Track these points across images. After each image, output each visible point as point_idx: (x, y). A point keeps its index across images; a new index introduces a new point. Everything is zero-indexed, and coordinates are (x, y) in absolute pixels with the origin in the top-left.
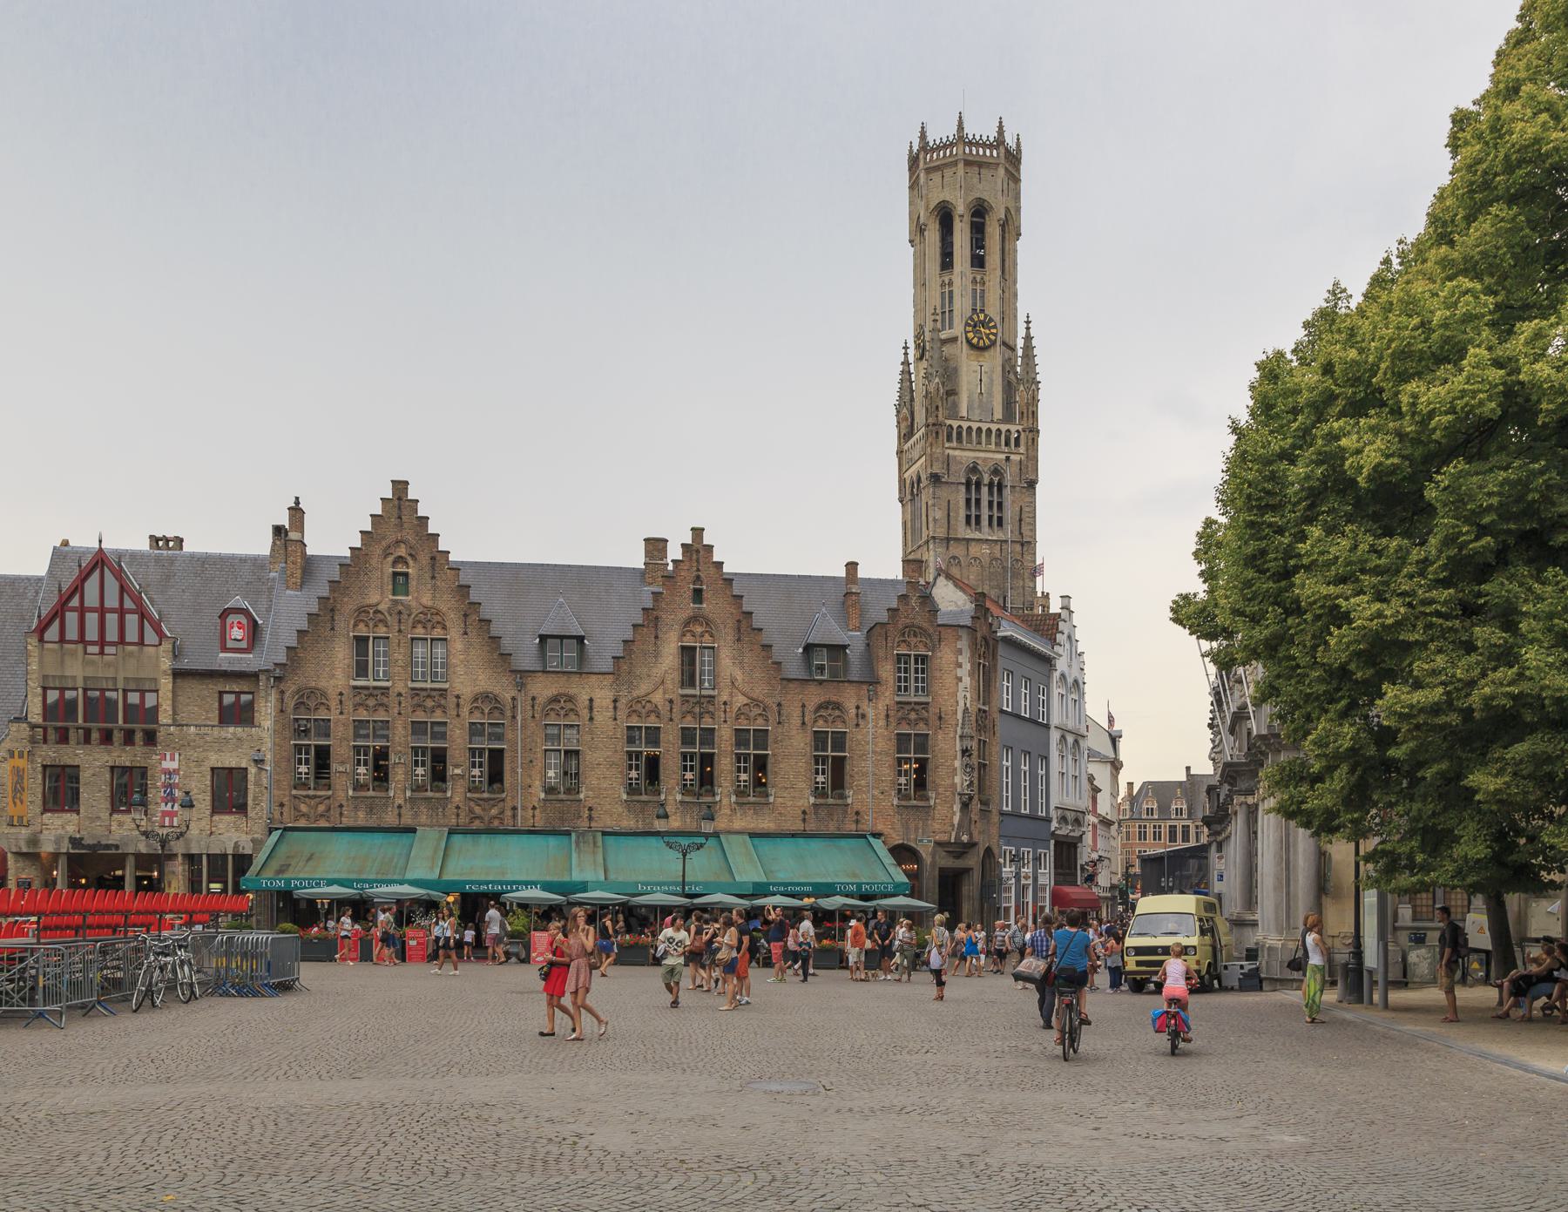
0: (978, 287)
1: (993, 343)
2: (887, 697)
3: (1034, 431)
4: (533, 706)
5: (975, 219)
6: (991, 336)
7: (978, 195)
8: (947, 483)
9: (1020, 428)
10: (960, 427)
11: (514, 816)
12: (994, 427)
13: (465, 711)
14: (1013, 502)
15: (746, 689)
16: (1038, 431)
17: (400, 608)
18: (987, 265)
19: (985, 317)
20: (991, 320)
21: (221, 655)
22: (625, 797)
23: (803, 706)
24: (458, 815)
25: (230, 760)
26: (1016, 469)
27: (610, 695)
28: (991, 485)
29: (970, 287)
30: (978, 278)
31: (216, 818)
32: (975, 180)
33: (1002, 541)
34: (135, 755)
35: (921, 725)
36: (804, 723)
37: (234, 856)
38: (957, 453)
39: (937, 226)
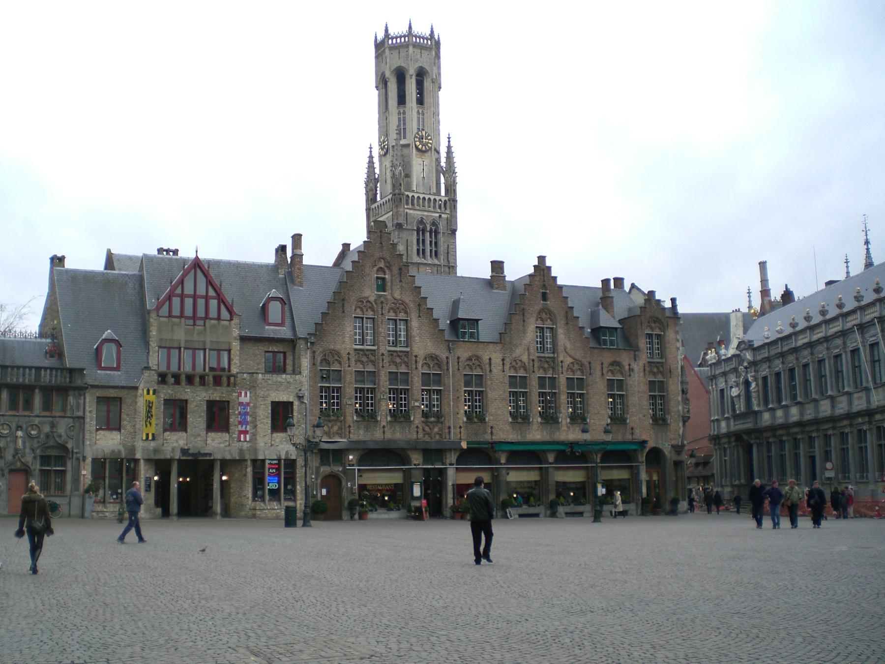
0: (421, 116)
2: (644, 359)
3: (454, 201)
4: (458, 363)
5: (418, 78)
7: (421, 65)
8: (406, 229)
9: (447, 199)
10: (413, 196)
11: (450, 432)
12: (432, 198)
13: (420, 365)
14: (444, 242)
15: (572, 353)
16: (457, 201)
17: (382, 299)
18: (425, 104)
21: (267, 327)
22: (510, 420)
23: (602, 364)
24: (417, 432)
25: (283, 397)
27: (501, 356)
28: (431, 232)
31: (275, 435)
32: (419, 56)
33: (438, 265)
34: (223, 393)
35: (660, 375)
36: (603, 374)
37: (285, 460)
38: (411, 212)
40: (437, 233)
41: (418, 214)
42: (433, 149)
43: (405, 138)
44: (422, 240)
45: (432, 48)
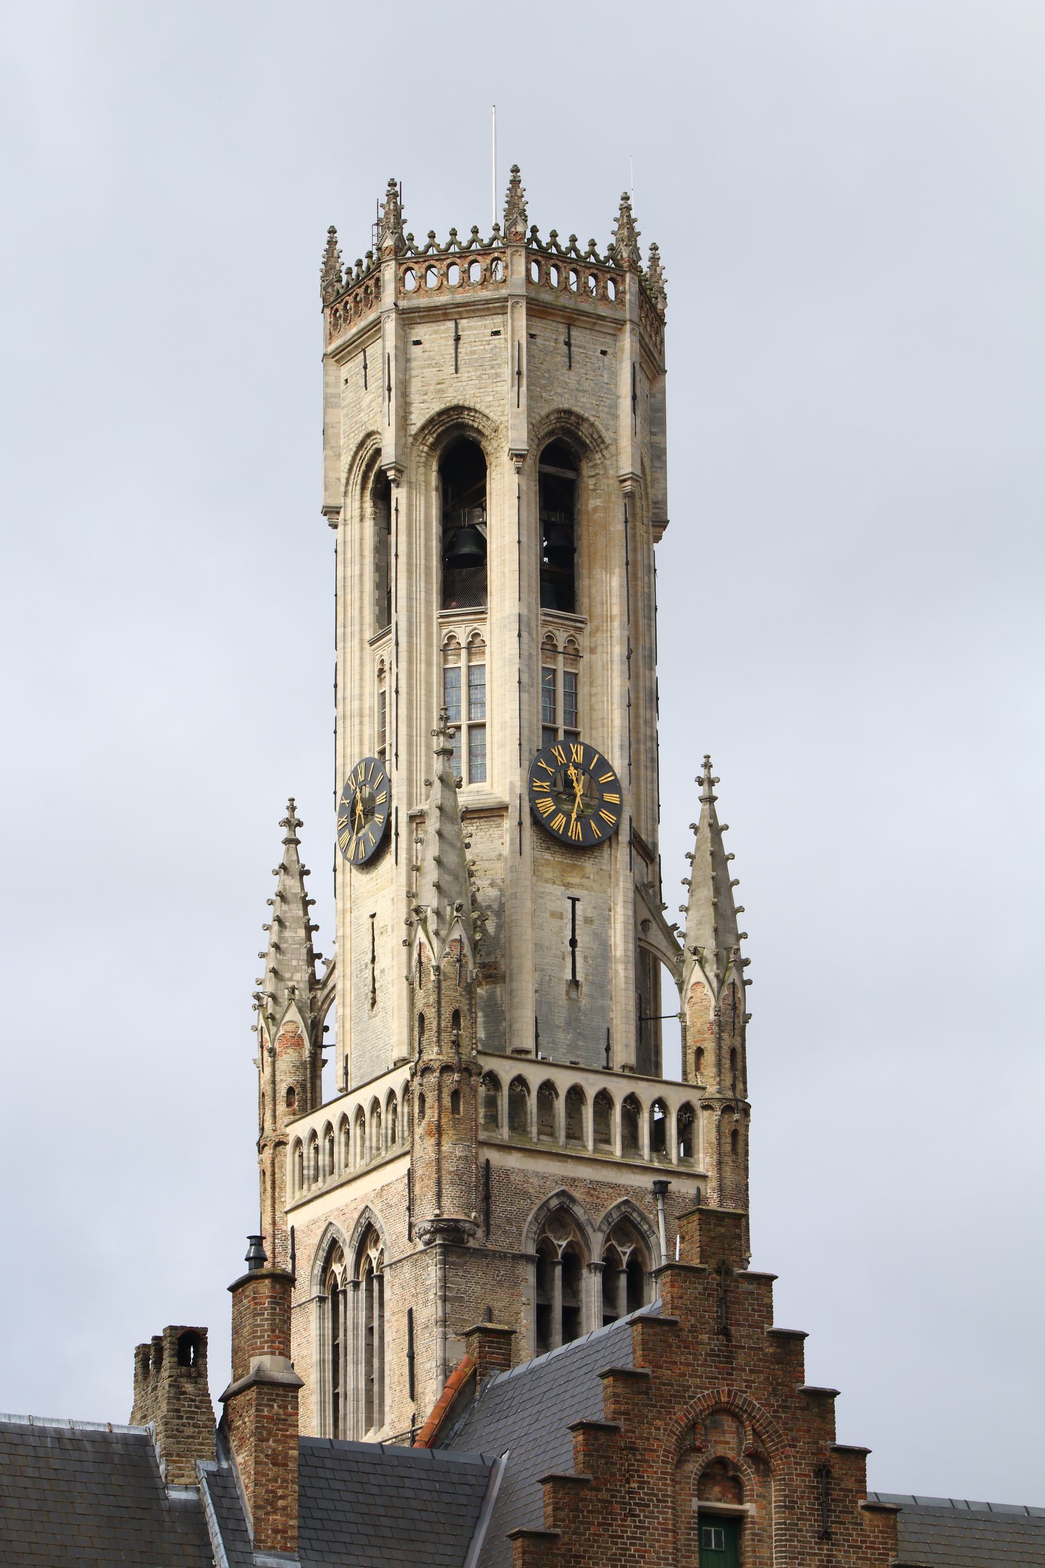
0: (560, 665)
1: (611, 835)
5: (549, 469)
8: (481, 1253)
10: (520, 1081)
12: (619, 1090)
16: (746, 1110)
18: (584, 601)
28: (609, 1269)
38: (513, 1161)
39: (434, 477)
41: (544, 1178)
42: (624, 837)
45: (620, 323)
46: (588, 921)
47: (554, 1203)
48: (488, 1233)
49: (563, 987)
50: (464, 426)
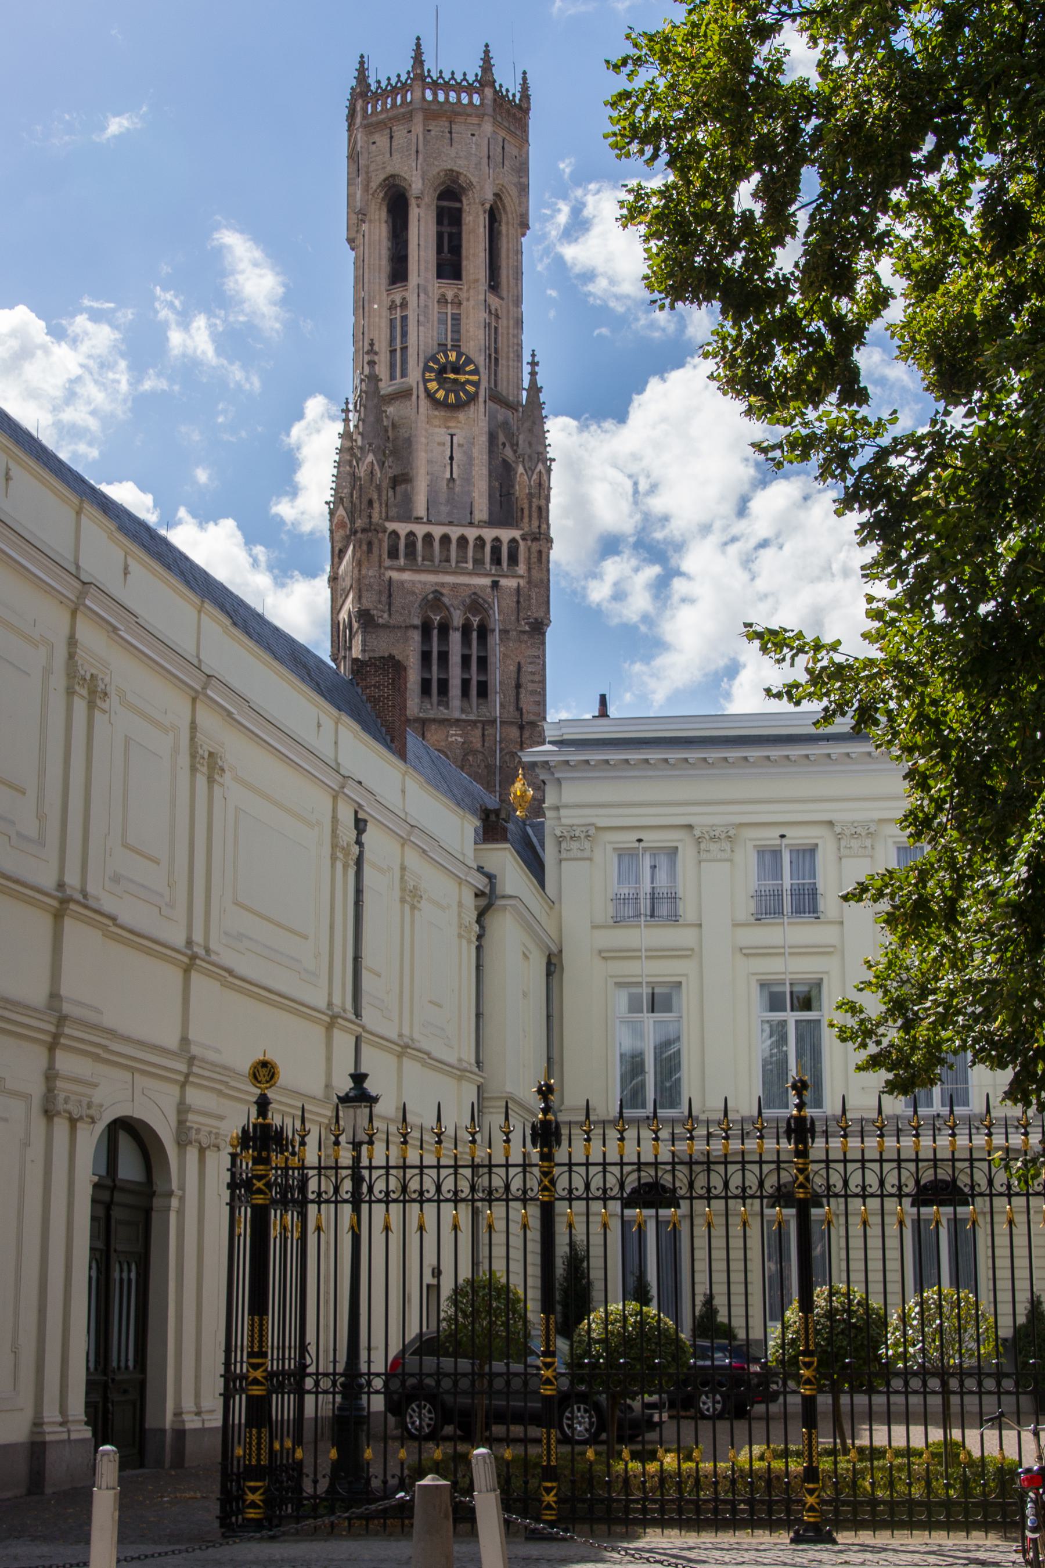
0: (449, 310)
1: (473, 398)
5: (445, 203)
6: (469, 388)
8: (385, 626)
9: (516, 534)
10: (411, 534)
12: (471, 534)
16: (550, 541)
18: (464, 273)
19: (459, 357)
20: (469, 361)
26: (510, 602)
28: (466, 630)
29: (435, 309)
30: (450, 295)
33: (484, 723)
38: (406, 576)
39: (384, 214)
40: (484, 632)
41: (425, 584)
43: (404, 375)
44: (439, 653)
46: (460, 445)
47: (431, 596)
48: (390, 615)
49: (445, 482)
50: (398, 186)
